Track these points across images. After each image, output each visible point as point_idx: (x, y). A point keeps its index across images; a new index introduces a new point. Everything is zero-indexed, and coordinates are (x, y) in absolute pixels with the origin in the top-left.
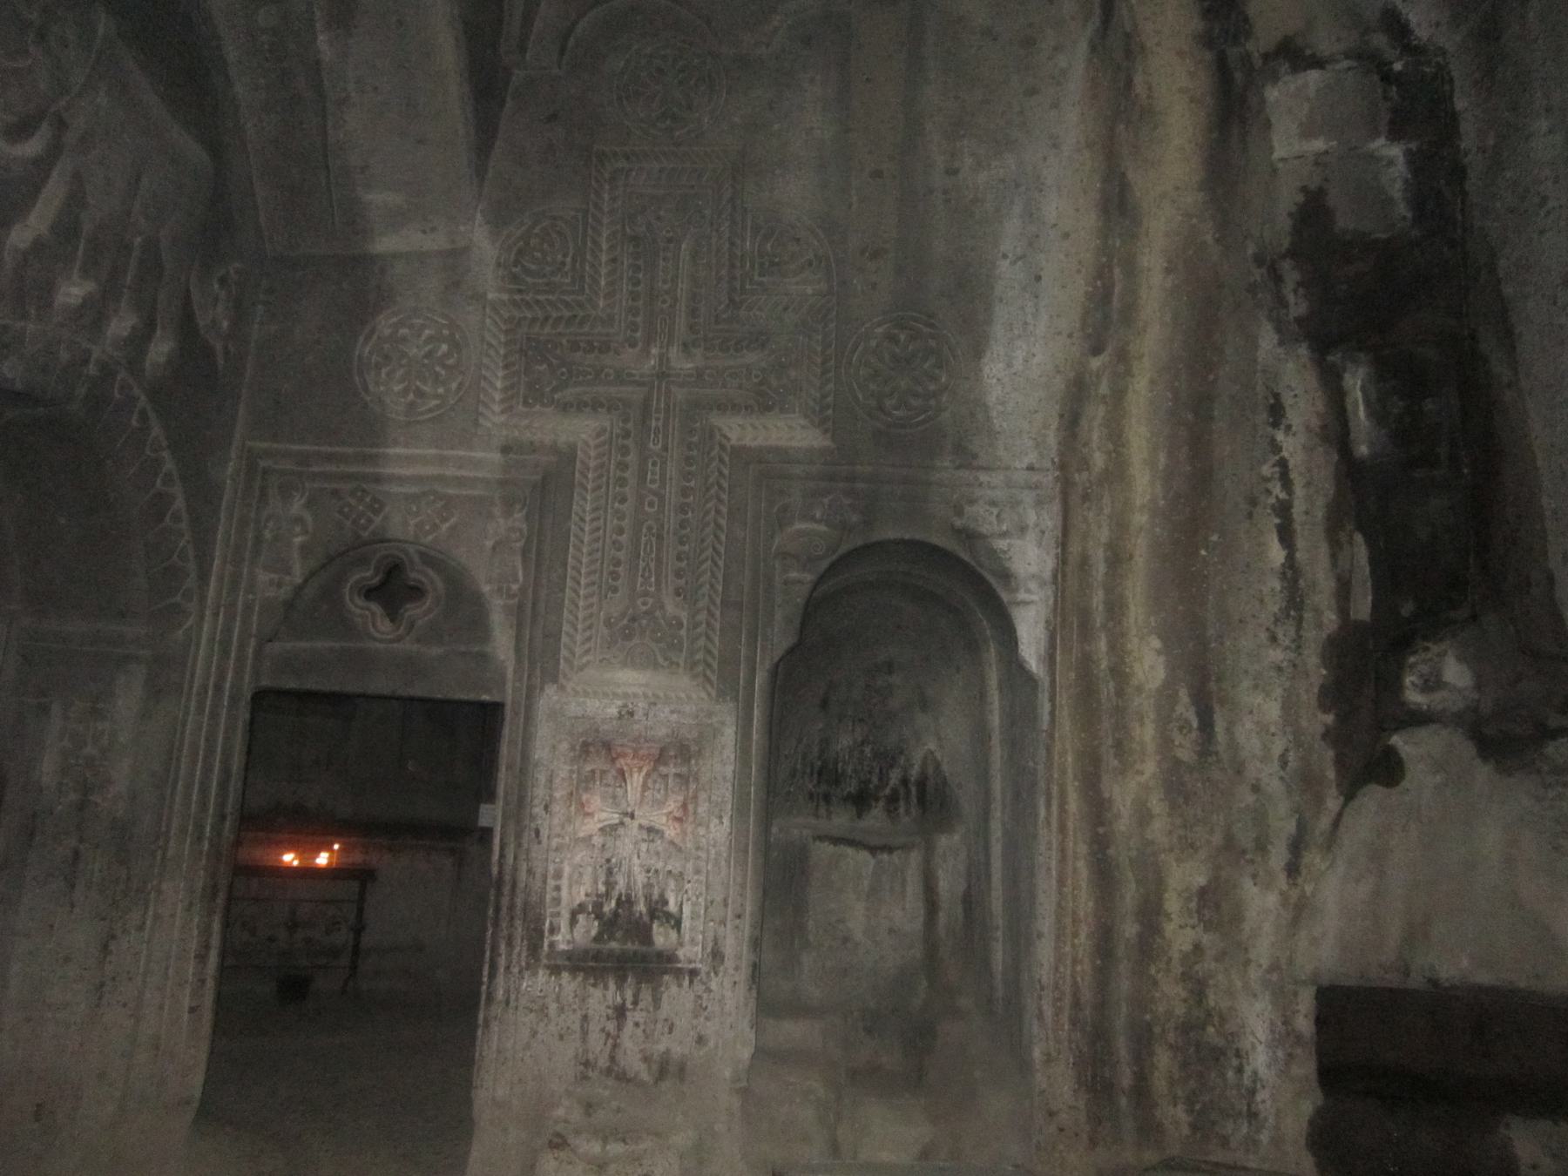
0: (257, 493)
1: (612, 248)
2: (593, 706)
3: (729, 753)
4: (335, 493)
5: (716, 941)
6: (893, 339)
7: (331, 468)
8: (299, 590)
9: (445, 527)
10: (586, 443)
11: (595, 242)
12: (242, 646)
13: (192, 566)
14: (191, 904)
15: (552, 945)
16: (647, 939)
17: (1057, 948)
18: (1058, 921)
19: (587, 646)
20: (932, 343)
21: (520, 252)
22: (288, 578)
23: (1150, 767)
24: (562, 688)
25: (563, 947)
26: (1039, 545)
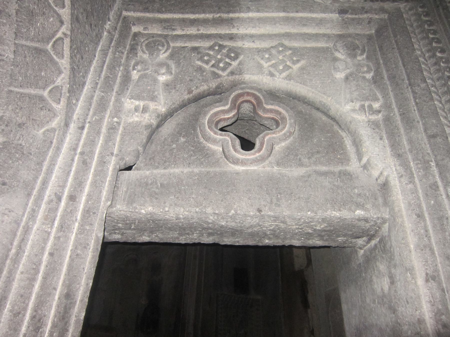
0: (128, 47)
4: (195, 49)
7: (192, 31)
9: (296, 67)
12: (102, 162)
22: (152, 106)
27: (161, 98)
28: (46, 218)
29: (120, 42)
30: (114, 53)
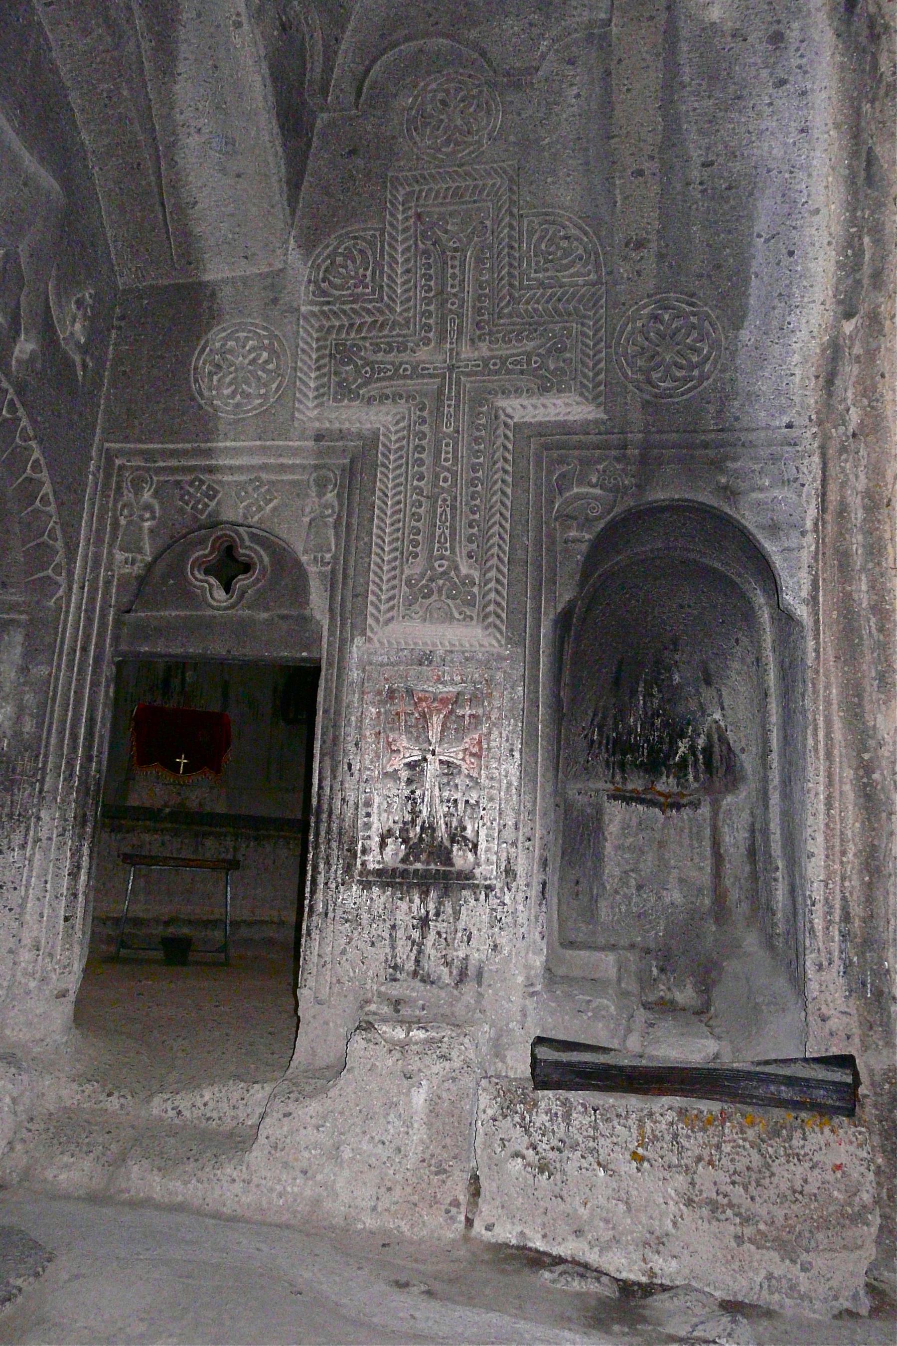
1: (407, 260)
4: (178, 483)
6: (656, 318)
7: (173, 463)
8: (149, 567)
11: (391, 256)
12: (103, 616)
13: (59, 544)
14: (64, 830)
15: (363, 864)
16: (449, 861)
17: (827, 867)
18: (827, 840)
19: (391, 603)
20: (694, 320)
22: (139, 557)
24: (370, 640)
27: (147, 548)
28: (67, 666)
29: (106, 485)
30: (101, 500)
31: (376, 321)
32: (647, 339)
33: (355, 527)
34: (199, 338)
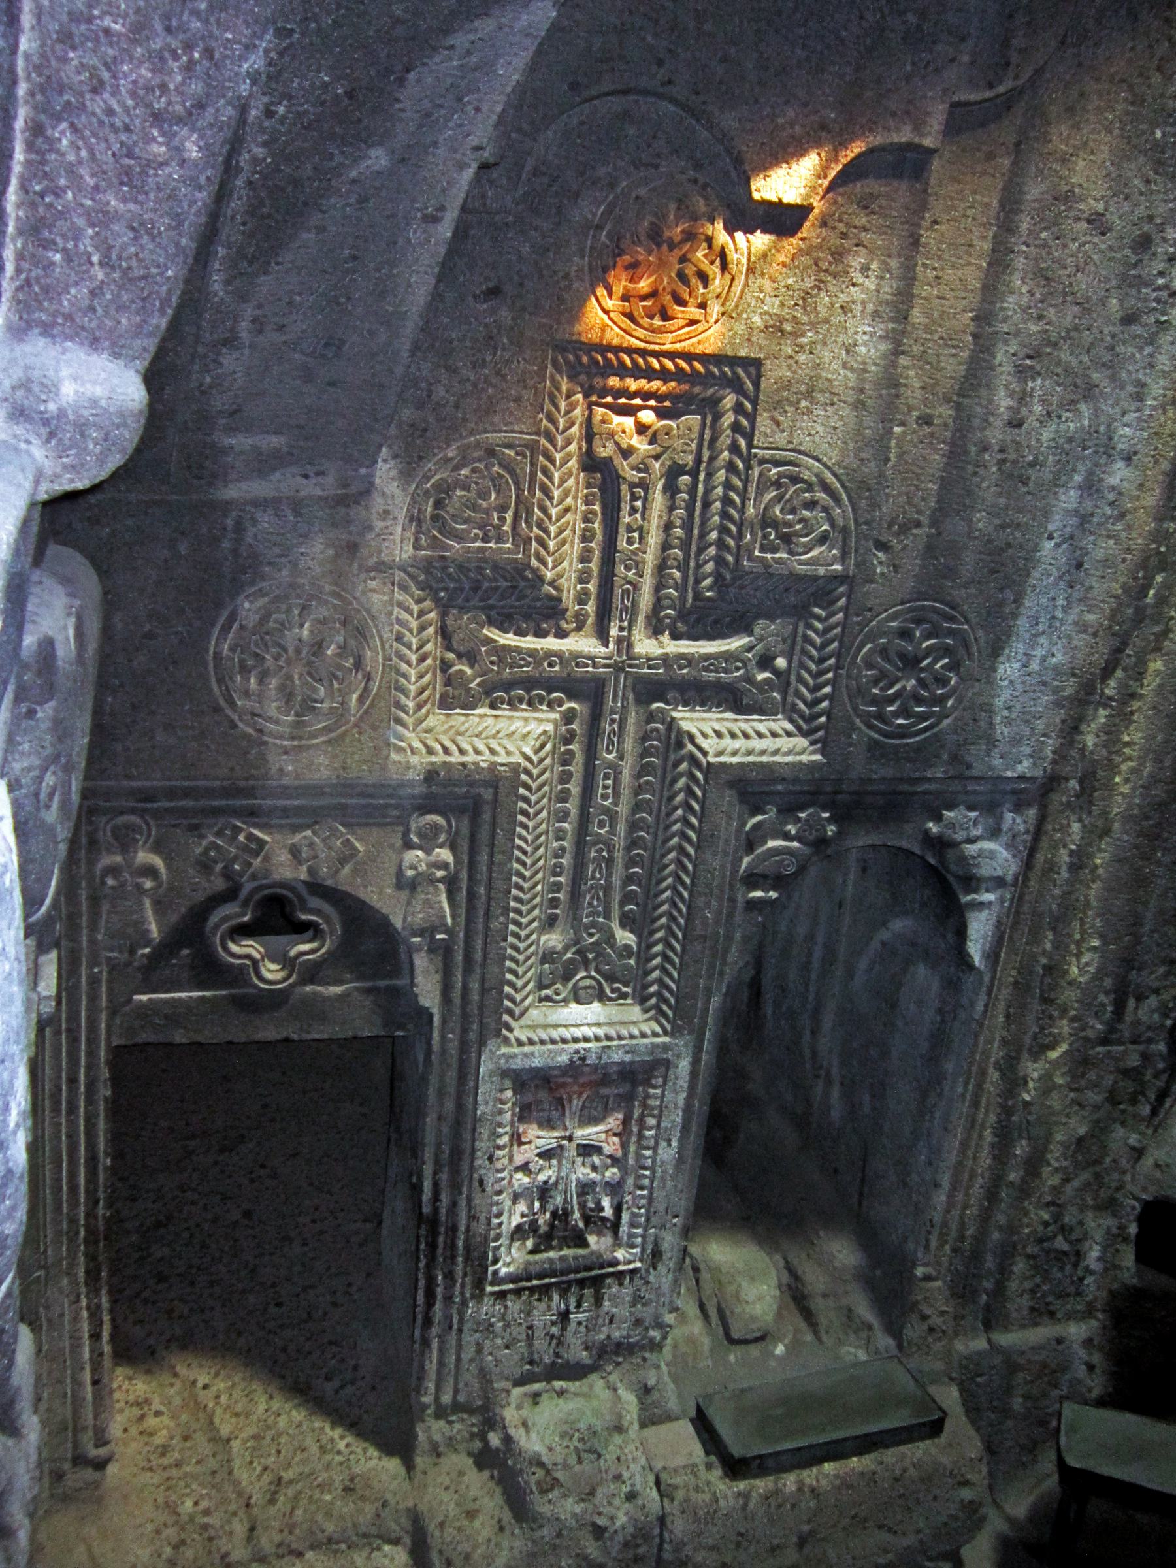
1: (566, 494)
2: (538, 1058)
3: (683, 1083)
5: (656, 1244)
10: (528, 758)
15: (496, 1273)
21: (438, 504)
23: (1064, 1047)
24: (506, 1041)
25: (504, 1271)
26: (1008, 847)
31: (515, 587)
32: (889, 661)
33: (484, 899)
34: (219, 605)
